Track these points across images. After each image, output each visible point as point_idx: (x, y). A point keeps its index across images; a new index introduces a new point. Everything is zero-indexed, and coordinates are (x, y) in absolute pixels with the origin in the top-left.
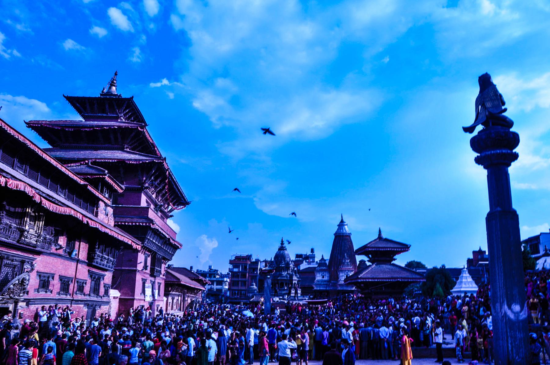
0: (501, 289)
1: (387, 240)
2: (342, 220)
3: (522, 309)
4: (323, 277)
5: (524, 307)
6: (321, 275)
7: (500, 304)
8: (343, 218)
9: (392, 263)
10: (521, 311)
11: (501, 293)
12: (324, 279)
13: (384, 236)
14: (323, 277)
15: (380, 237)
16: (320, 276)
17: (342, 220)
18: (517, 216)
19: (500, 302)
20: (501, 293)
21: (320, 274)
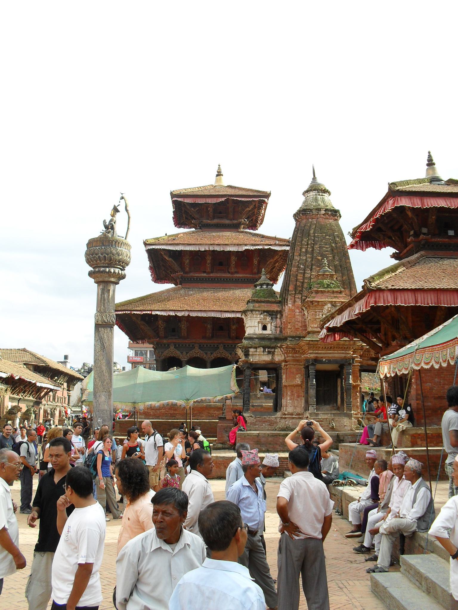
2: (314, 178)
4: (265, 328)
6: (259, 323)
12: (265, 332)
14: (265, 328)
16: (256, 324)
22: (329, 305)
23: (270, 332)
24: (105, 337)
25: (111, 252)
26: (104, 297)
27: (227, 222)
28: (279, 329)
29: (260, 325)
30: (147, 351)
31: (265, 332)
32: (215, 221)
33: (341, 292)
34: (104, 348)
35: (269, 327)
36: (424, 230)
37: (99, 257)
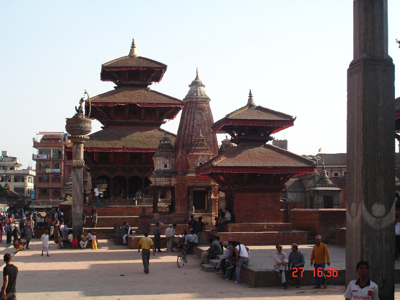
0: (359, 180)
1: (260, 108)
2: (197, 78)
3: (388, 210)
4: (166, 166)
5: (390, 209)
6: (162, 163)
7: (357, 204)
8: (198, 75)
9: (267, 143)
10: (385, 216)
11: (359, 187)
12: (166, 169)
13: (257, 102)
14: (166, 166)
15: (250, 105)
17: (197, 78)
18: (393, 66)
19: (357, 200)
20: (359, 187)
21: (161, 162)
22: (201, 157)
23: (169, 169)
24: (79, 173)
25: (82, 127)
26: (78, 151)
27: (139, 83)
28: (174, 167)
29: (164, 165)
30: (50, 149)
31: (166, 169)
32: (131, 82)
33: (208, 149)
34: (79, 180)
35: (168, 165)
36: (243, 134)
37: (75, 129)
